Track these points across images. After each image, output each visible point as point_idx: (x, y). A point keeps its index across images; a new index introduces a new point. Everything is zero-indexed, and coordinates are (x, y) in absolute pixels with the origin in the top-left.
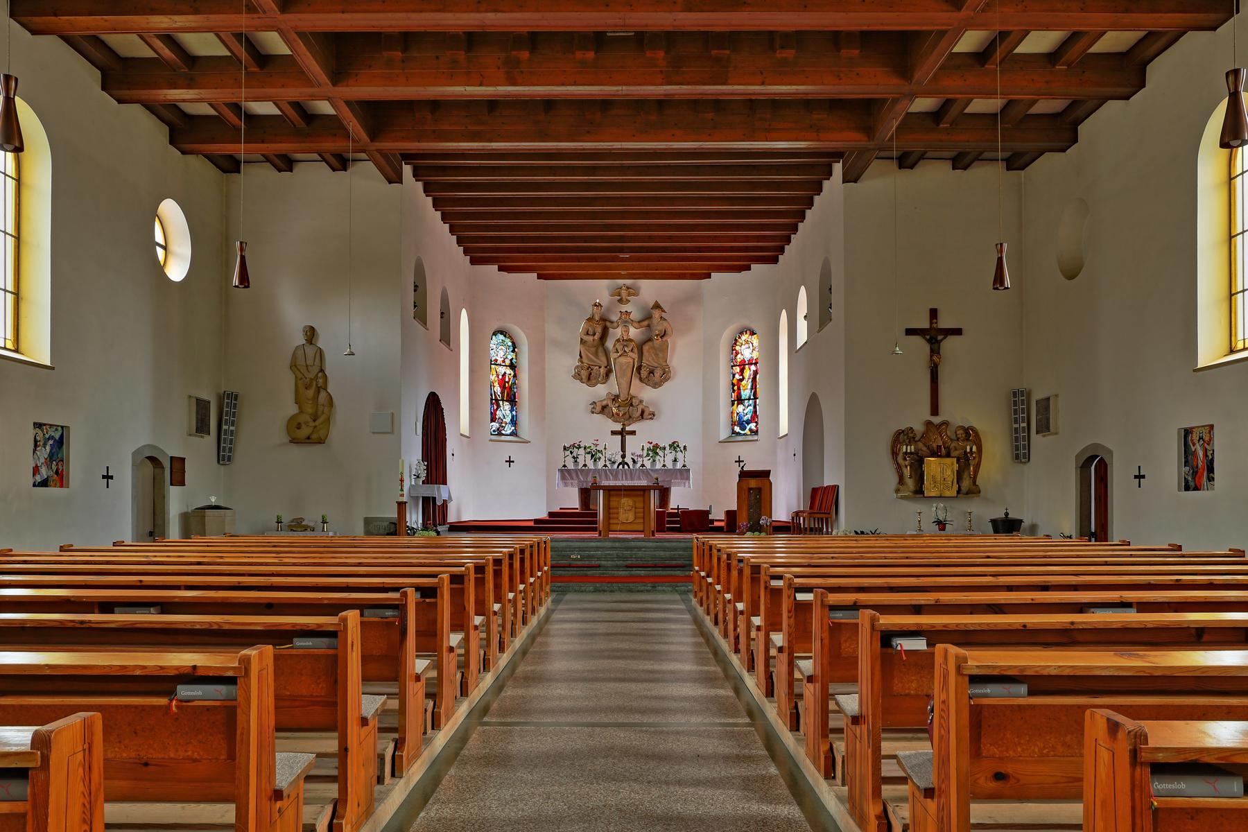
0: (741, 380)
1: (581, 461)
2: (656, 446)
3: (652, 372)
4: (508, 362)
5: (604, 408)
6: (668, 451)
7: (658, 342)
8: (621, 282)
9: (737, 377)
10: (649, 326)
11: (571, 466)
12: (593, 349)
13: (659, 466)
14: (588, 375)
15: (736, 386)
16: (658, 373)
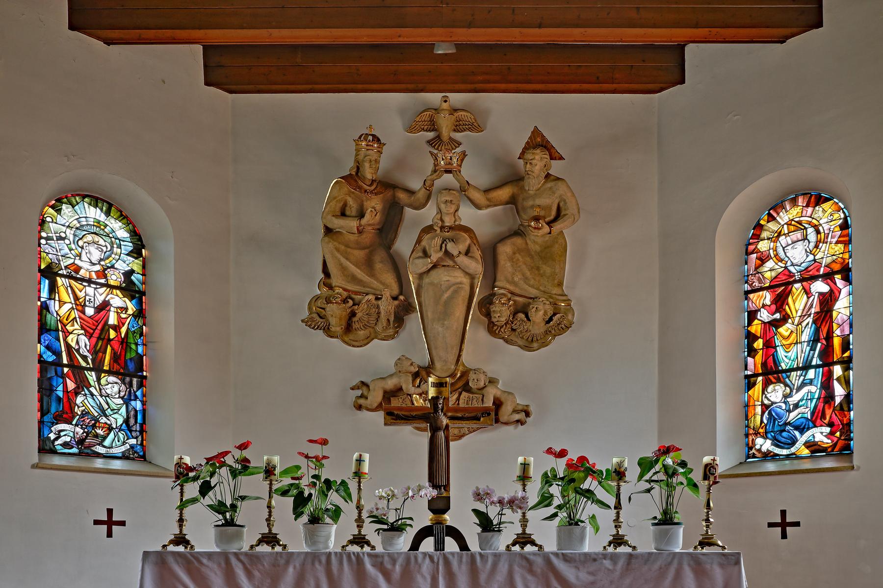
0: (776, 324)
1: (252, 522)
2: (582, 467)
3: (524, 310)
4: (115, 278)
5: (389, 395)
6: (632, 485)
7: (539, 235)
8: (434, 98)
9: (764, 316)
10: (512, 201)
11: (204, 537)
12: (360, 254)
13: (592, 543)
14: (343, 317)
15: (760, 343)
16: (538, 315)
